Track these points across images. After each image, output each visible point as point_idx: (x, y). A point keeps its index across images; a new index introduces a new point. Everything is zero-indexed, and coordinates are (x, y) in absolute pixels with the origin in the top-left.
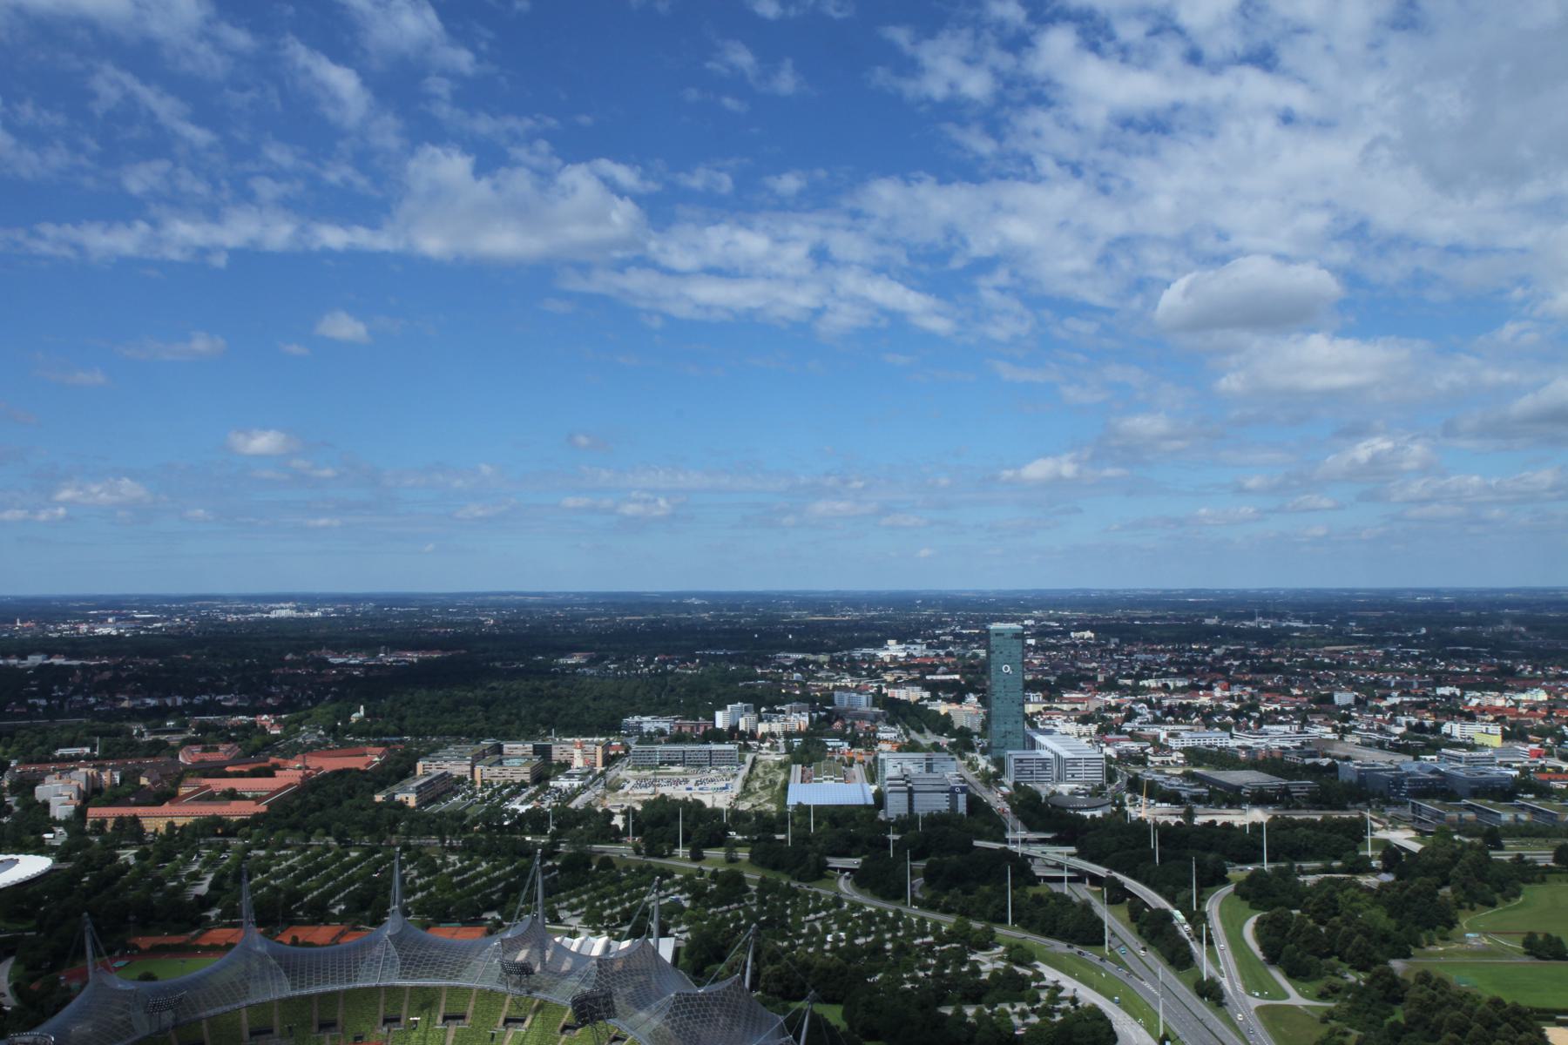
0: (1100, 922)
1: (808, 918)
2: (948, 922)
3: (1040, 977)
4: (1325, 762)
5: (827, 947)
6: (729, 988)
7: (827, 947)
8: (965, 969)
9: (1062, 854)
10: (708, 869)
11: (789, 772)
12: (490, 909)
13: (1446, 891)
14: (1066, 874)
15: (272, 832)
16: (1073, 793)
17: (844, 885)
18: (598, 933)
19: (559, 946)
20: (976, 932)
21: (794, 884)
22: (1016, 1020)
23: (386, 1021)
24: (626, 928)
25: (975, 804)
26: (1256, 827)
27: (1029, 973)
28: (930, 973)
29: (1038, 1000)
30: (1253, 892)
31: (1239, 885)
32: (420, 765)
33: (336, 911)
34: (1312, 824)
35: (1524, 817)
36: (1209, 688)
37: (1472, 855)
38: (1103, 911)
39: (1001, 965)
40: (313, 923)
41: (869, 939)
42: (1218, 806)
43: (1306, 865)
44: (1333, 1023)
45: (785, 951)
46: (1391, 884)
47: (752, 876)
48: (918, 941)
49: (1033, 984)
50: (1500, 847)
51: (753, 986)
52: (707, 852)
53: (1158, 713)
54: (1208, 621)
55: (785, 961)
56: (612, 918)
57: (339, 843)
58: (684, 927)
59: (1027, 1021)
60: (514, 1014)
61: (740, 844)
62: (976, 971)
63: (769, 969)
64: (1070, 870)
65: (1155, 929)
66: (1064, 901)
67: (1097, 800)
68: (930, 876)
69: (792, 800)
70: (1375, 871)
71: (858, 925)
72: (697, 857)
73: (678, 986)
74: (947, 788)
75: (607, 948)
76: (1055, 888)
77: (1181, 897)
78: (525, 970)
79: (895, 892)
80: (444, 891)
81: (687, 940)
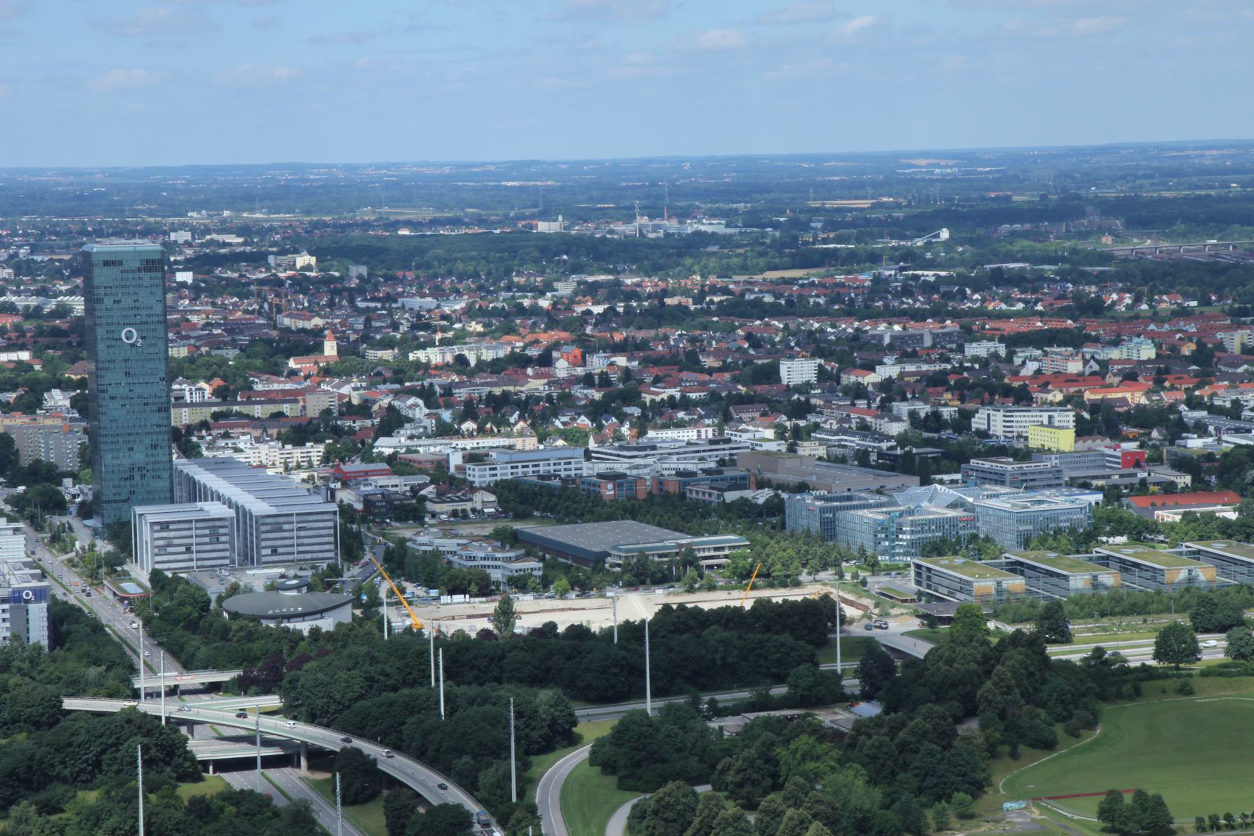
4: (762, 496)
13: (971, 727)
16: (272, 588)
26: (631, 631)
31: (599, 745)
34: (729, 617)
35: (1109, 578)
36: (546, 360)
37: (1015, 656)
42: (563, 595)
43: (725, 698)
46: (876, 722)
50: (1065, 638)
53: (446, 415)
54: (543, 227)
64: (267, 743)
67: (322, 598)
70: (847, 700)
77: (487, 777)
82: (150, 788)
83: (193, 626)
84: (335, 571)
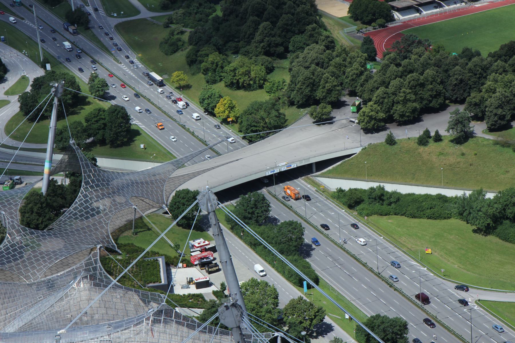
44: (173, 26)
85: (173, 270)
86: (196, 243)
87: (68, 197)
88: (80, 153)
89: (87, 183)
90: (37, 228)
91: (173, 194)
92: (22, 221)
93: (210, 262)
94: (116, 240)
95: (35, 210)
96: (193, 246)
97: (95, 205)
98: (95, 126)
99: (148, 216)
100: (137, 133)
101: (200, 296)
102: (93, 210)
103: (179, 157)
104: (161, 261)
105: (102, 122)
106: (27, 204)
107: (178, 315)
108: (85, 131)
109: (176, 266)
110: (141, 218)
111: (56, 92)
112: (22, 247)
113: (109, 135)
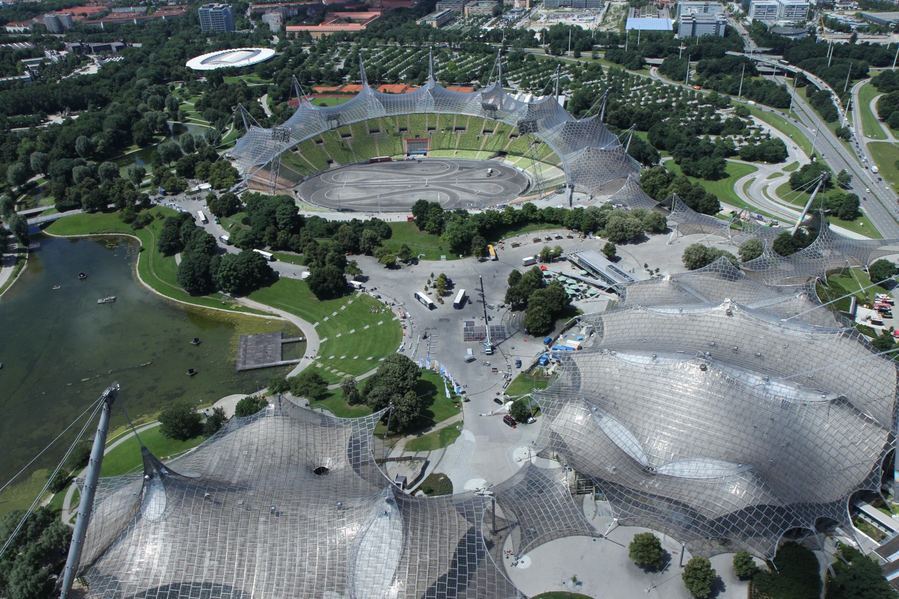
0: (789, 96)
1: (633, 89)
2: (706, 93)
3: (752, 123)
5: (642, 103)
6: (593, 120)
7: (642, 103)
8: (712, 118)
9: (775, 60)
10: (583, 62)
11: (628, 11)
12: (475, 78)
14: (774, 70)
15: (370, 39)
16: (786, 26)
17: (653, 73)
18: (527, 92)
19: (509, 97)
20: (721, 99)
21: (627, 71)
22: (736, 144)
23: (429, 129)
24: (541, 90)
25: (729, 31)
27: (746, 121)
28: (694, 118)
29: (749, 134)
30: (878, 84)
32: (437, 6)
33: (402, 78)
38: (791, 90)
39: (731, 116)
40: (393, 83)
41: (664, 101)
45: (621, 104)
47: (606, 67)
48: (689, 103)
49: (748, 126)
51: (605, 121)
52: (582, 53)
55: (620, 109)
56: (534, 85)
57: (401, 45)
58: (570, 91)
59: (742, 144)
60: (487, 129)
61: (599, 50)
62: (719, 119)
63: (612, 113)
64: (778, 68)
65: (820, 102)
66: (772, 85)
67: (799, 30)
68: (699, 70)
69: (629, 27)
71: (659, 93)
72: (577, 56)
73: (567, 118)
74: (715, 22)
75: (532, 100)
76: (767, 78)
77: (838, 84)
78: (493, 108)
79: (681, 78)
80: (452, 70)
81: (571, 97)
82: (744, 77)
83: (762, 35)
84: (804, 23)
85: (859, 308)
86: (880, 296)
87: (806, 242)
88: (822, 217)
89: (821, 237)
90: (781, 254)
91: (876, 260)
92: (773, 248)
93: (887, 311)
94: (827, 277)
95: (784, 243)
96: (878, 297)
97: (821, 252)
98: (834, 203)
99: (853, 269)
100: (861, 214)
101: (873, 329)
102: (819, 254)
103: (886, 238)
104: (853, 299)
105: (840, 202)
106: (780, 239)
107: (861, 338)
108: (827, 204)
109: (862, 305)
110: (848, 269)
111: (823, 177)
112: (769, 263)
113: (841, 211)
